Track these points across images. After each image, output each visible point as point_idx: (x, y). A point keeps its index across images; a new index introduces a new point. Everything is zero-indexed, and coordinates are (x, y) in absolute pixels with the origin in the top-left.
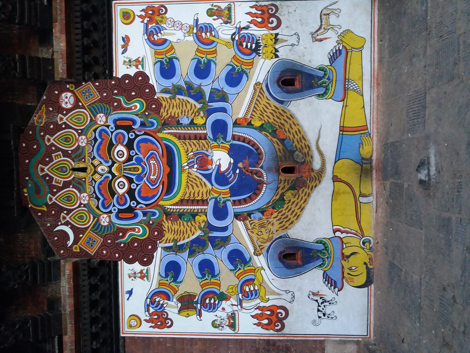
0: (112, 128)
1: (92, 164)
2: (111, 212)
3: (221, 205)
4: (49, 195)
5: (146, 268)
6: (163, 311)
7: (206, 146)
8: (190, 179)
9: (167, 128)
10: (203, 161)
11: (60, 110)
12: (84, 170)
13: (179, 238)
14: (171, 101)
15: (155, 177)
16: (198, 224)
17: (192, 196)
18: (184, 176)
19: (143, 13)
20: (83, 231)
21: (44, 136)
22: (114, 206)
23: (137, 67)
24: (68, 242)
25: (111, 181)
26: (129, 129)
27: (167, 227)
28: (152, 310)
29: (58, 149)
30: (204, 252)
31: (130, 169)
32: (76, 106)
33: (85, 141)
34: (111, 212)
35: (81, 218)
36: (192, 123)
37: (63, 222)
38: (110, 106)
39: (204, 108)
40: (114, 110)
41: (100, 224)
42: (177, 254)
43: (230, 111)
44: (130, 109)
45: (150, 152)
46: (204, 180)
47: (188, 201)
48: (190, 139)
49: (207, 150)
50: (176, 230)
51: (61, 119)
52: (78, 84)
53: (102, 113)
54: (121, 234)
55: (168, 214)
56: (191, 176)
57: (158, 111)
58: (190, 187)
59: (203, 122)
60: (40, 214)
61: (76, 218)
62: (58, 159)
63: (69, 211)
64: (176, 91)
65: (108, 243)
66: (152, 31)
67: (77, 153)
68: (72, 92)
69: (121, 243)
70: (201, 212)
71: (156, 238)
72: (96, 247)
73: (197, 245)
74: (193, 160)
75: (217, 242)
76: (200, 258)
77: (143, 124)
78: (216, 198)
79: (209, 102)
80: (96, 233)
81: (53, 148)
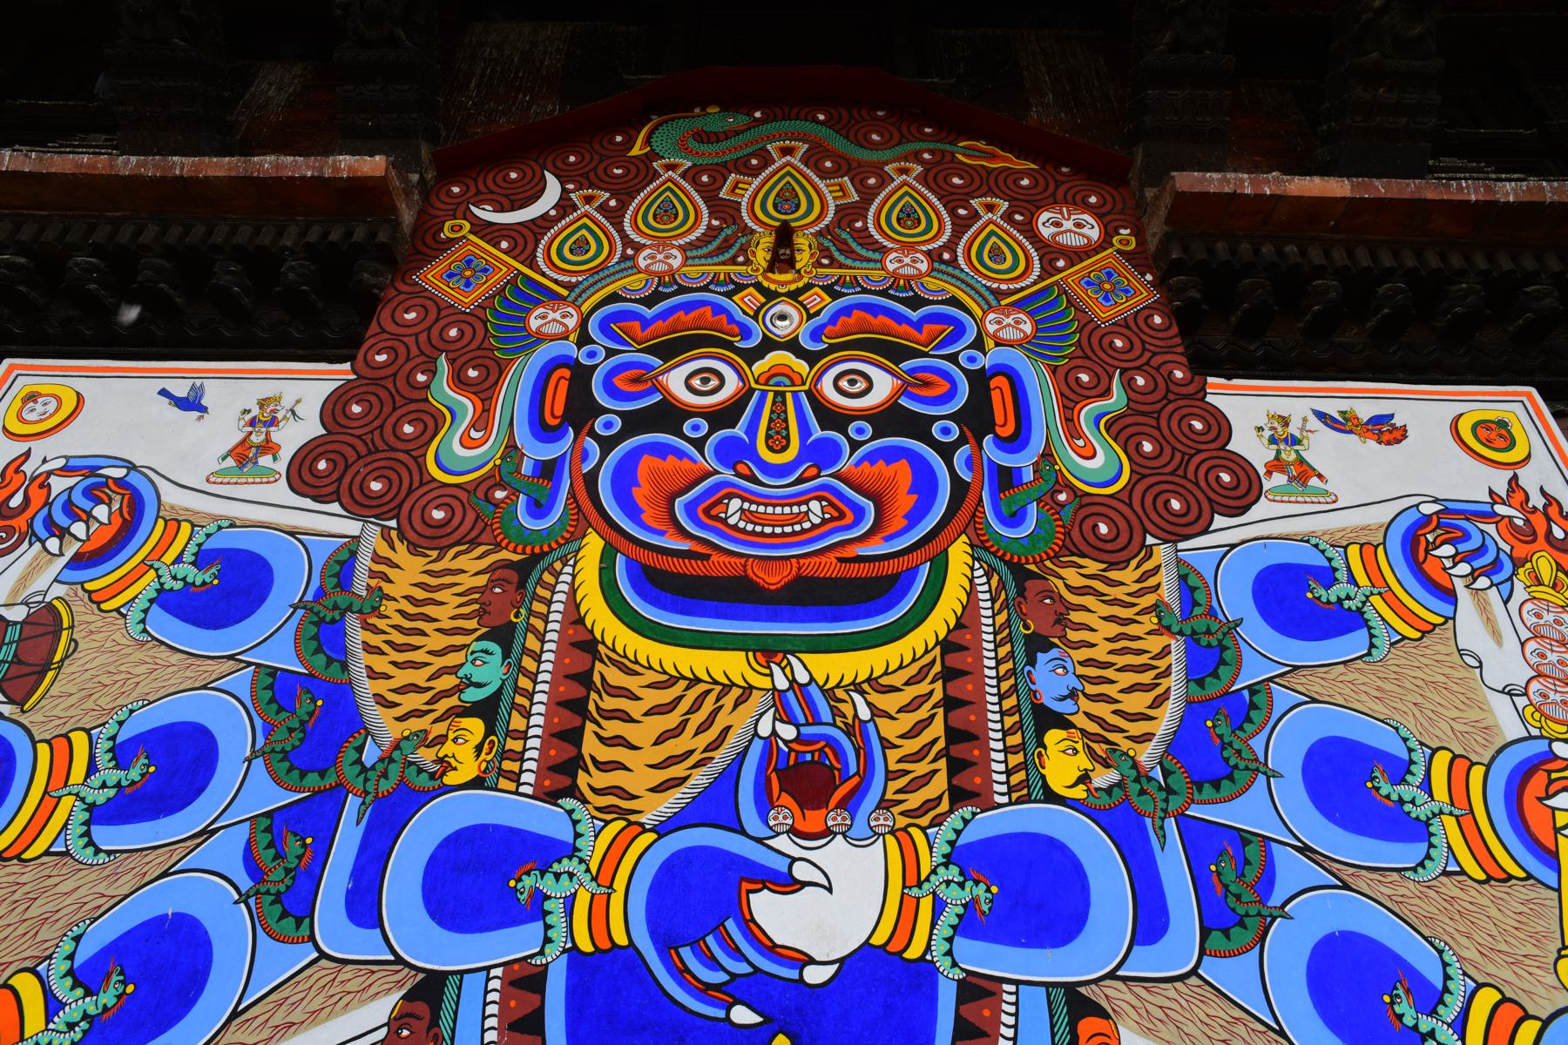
1: (808, 287)
2: (584, 339)
5: (282, 466)
6: (31, 535)
7: (914, 800)
8: (712, 698)
9: (1002, 585)
10: (814, 781)
11: (1026, 207)
12: (782, 258)
13: (381, 624)
15: (732, 521)
16: (440, 729)
17: (609, 703)
19: (1537, 501)
22: (611, 353)
23: (1277, 465)
25: (729, 346)
26: (976, 420)
27: (455, 565)
28: (58, 485)
30: (259, 763)
32: (1050, 252)
34: (584, 339)
36: (1047, 719)
37: (572, 195)
38: (1071, 357)
39: (1142, 792)
41: (538, 303)
42: (300, 612)
43: (1145, 963)
44: (1073, 431)
45: (870, 506)
46: (700, 779)
47: (585, 678)
48: (950, 703)
49: (884, 804)
50: (429, 610)
51: (990, 208)
55: (522, 574)
56: (729, 701)
57: (1085, 548)
59: (1057, 786)
65: (449, 325)
66: (1466, 536)
68: (1105, 243)
69: (432, 373)
73: (313, 721)
74: (826, 715)
75: (293, 847)
76: (235, 732)
77: (1006, 479)
78: (572, 851)
79: (1184, 822)
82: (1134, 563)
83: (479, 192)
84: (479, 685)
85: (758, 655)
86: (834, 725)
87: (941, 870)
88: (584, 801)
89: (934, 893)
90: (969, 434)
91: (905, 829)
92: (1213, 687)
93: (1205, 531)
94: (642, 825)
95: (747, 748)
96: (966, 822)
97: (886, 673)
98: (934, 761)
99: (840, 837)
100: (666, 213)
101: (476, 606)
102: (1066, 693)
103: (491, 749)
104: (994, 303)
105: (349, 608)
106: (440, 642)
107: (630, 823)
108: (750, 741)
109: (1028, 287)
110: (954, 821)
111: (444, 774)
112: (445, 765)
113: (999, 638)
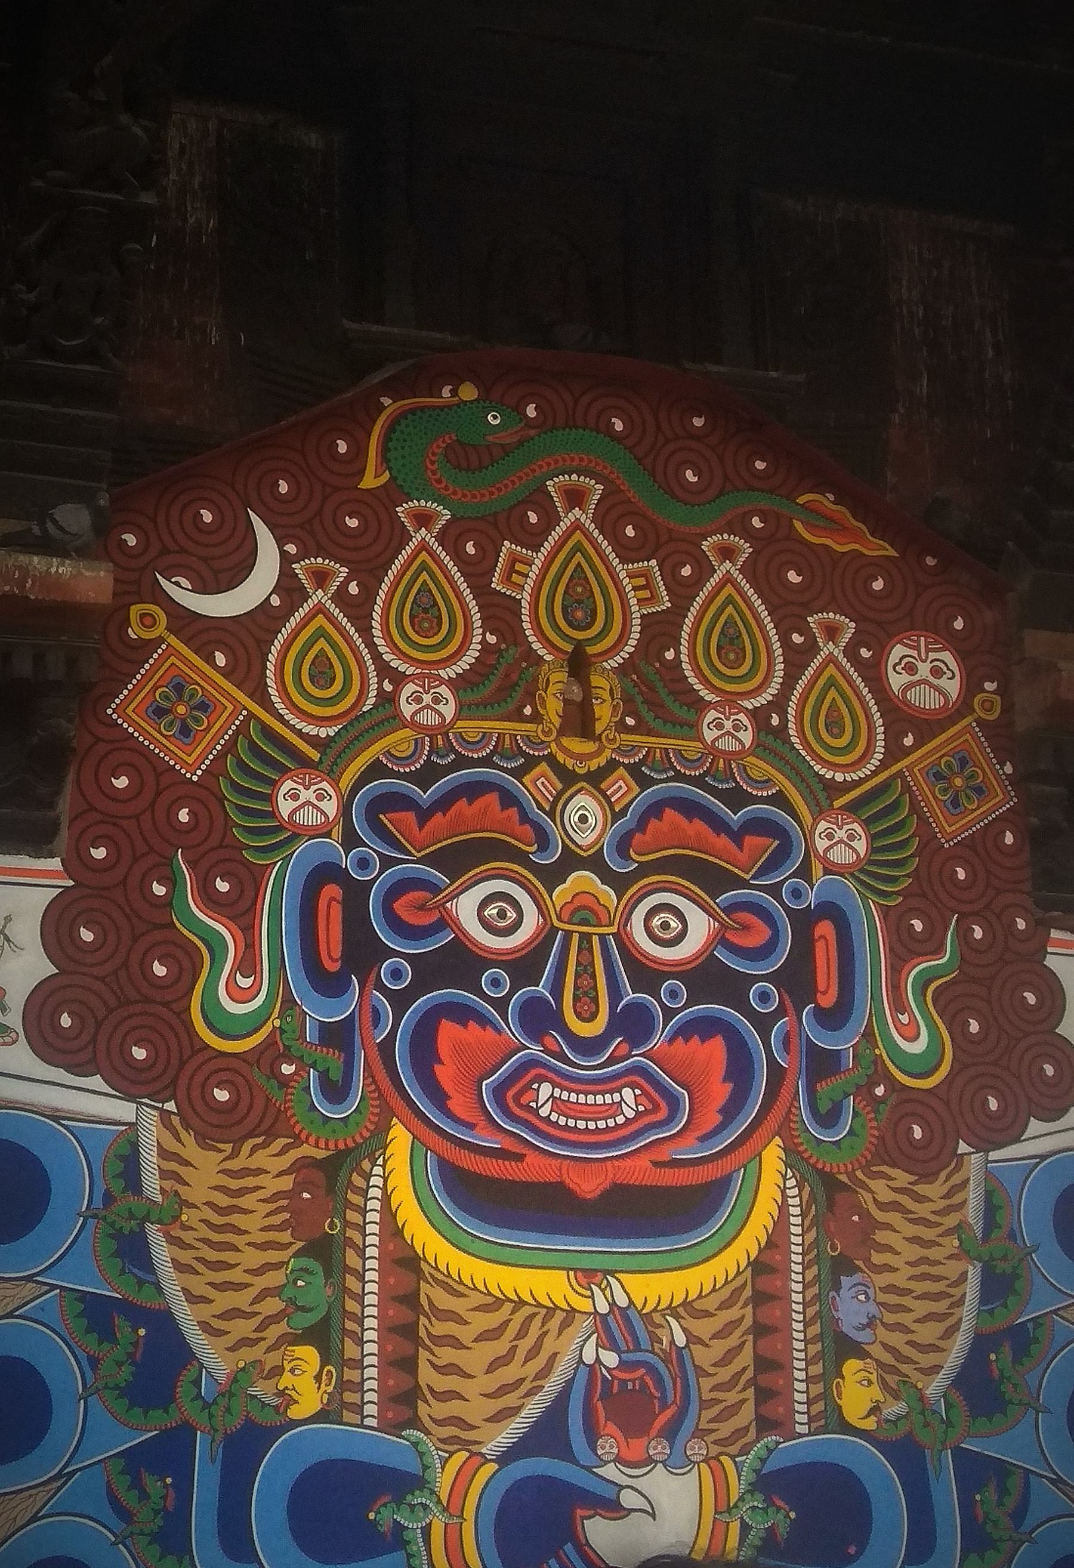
0: (796, 894)
1: (612, 765)
3: (384, 1515)
4: (447, 515)
7: (725, 1429)
8: (537, 1321)
11: (877, 631)
12: (579, 720)
13: (188, 1237)
14: (948, 1233)
15: (544, 1112)
17: (440, 1328)
18: (550, 1286)
20: (248, 674)
21: (748, 534)
22: (387, 862)
24: (185, 583)
25: (521, 857)
29: (683, 593)
31: (585, 970)
32: (899, 716)
33: (728, 745)
34: (351, 840)
35: (322, 673)
39: (927, 1425)
40: (886, 912)
41: (283, 770)
44: (899, 1006)
46: (533, 1409)
47: (411, 1300)
48: (760, 1330)
49: (699, 1433)
50: (235, 1219)
51: (832, 632)
52: (1000, 736)
53: (873, 850)
54: (223, 886)
56: (554, 1324)
58: (491, 1320)
60: (342, 447)
61: (322, 643)
62: (632, 590)
63: (358, 610)
64: (1001, 1267)
67: (663, 693)
68: (964, 706)
69: (171, 881)
70: (343, 1385)
71: (196, 1093)
72: (157, 740)
74: (645, 1343)
77: (822, 1064)
80: (231, 747)
81: (686, 571)
82: (943, 1175)
83: (165, 551)
84: (304, 1309)
85: (579, 1274)
86: (652, 1352)
87: (748, 1497)
88: (428, 1433)
89: (742, 1518)
90: (788, 1002)
91: (716, 1458)
92: (1001, 1320)
93: (1017, 1140)
94: (483, 1455)
95: (575, 1374)
96: (770, 1451)
97: (700, 1296)
98: (744, 1389)
99: (660, 1465)
100: (425, 614)
101: (287, 1216)
102: (865, 1321)
103: (330, 1380)
104: (824, 804)
105: (147, 1218)
106: (254, 1258)
107: (472, 1454)
108: (576, 1369)
109: (868, 778)
110: (758, 1448)
111: (287, 1406)
112: (286, 1398)
113: (807, 1259)
